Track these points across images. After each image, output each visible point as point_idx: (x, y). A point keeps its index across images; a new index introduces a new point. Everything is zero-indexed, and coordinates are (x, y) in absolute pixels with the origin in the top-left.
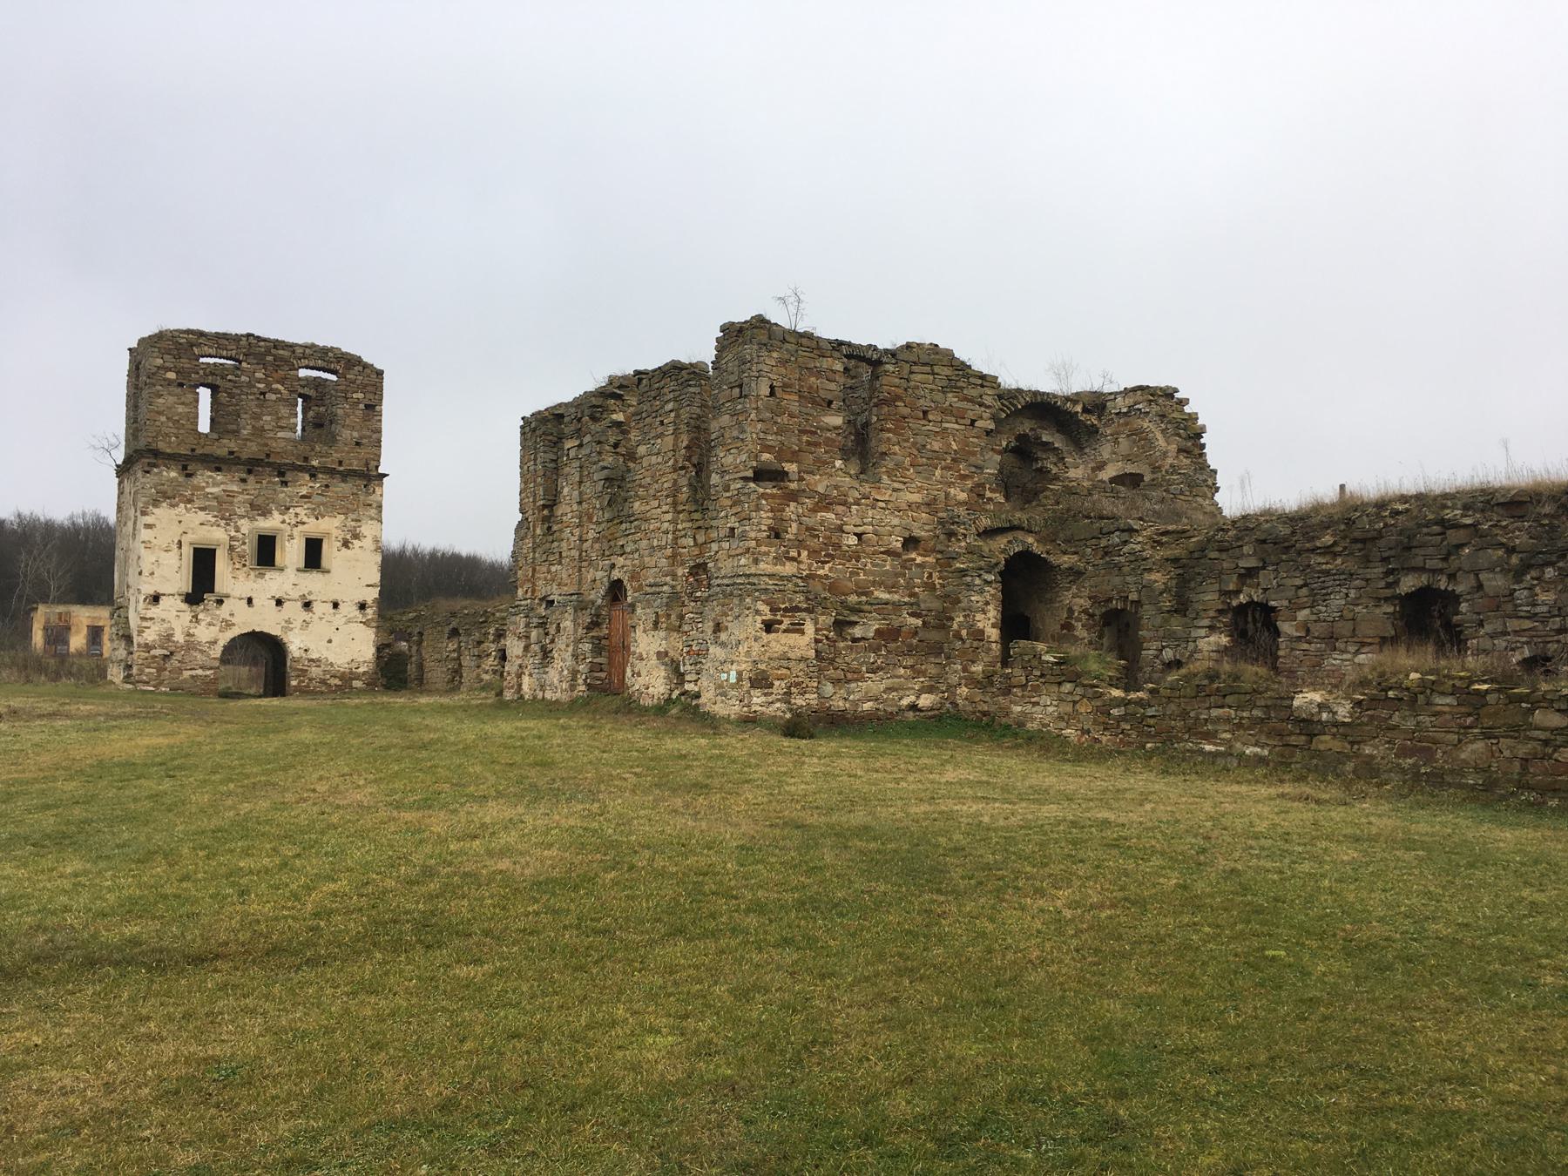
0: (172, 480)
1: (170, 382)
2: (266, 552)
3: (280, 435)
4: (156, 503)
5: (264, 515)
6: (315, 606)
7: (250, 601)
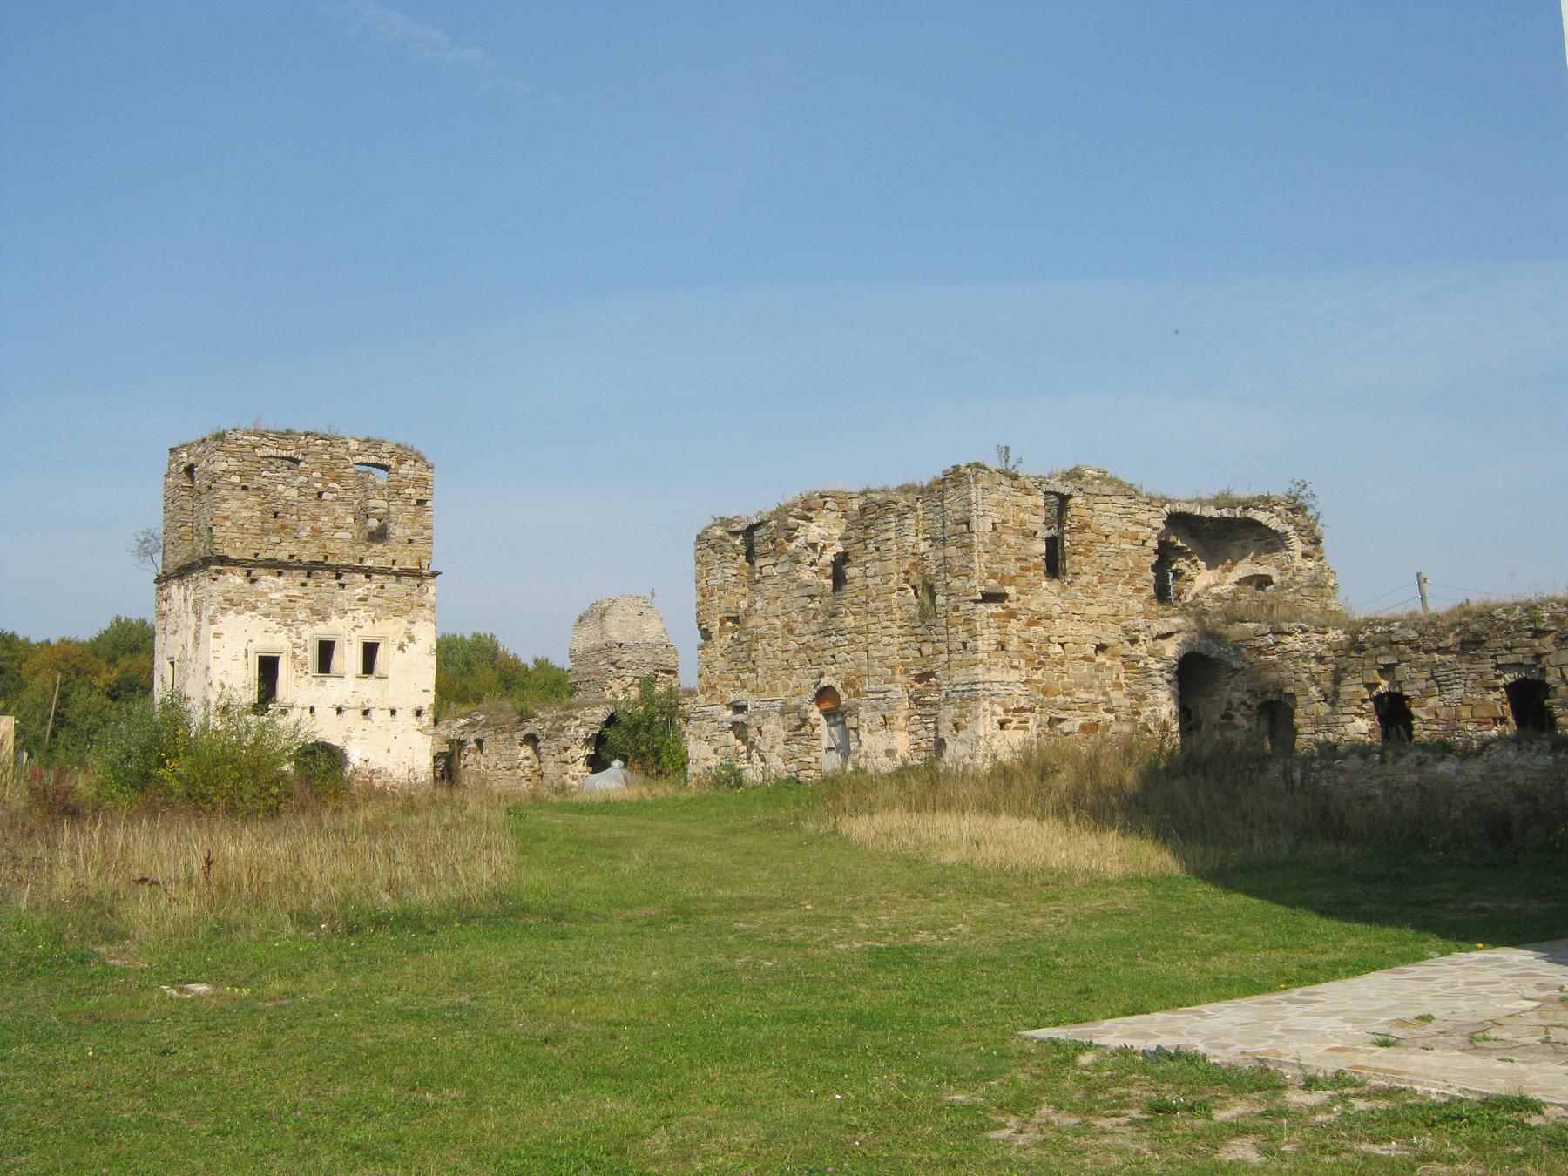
0: (238, 586)
1: (234, 486)
3: (337, 536)
4: (224, 610)
5: (323, 620)
6: (372, 712)
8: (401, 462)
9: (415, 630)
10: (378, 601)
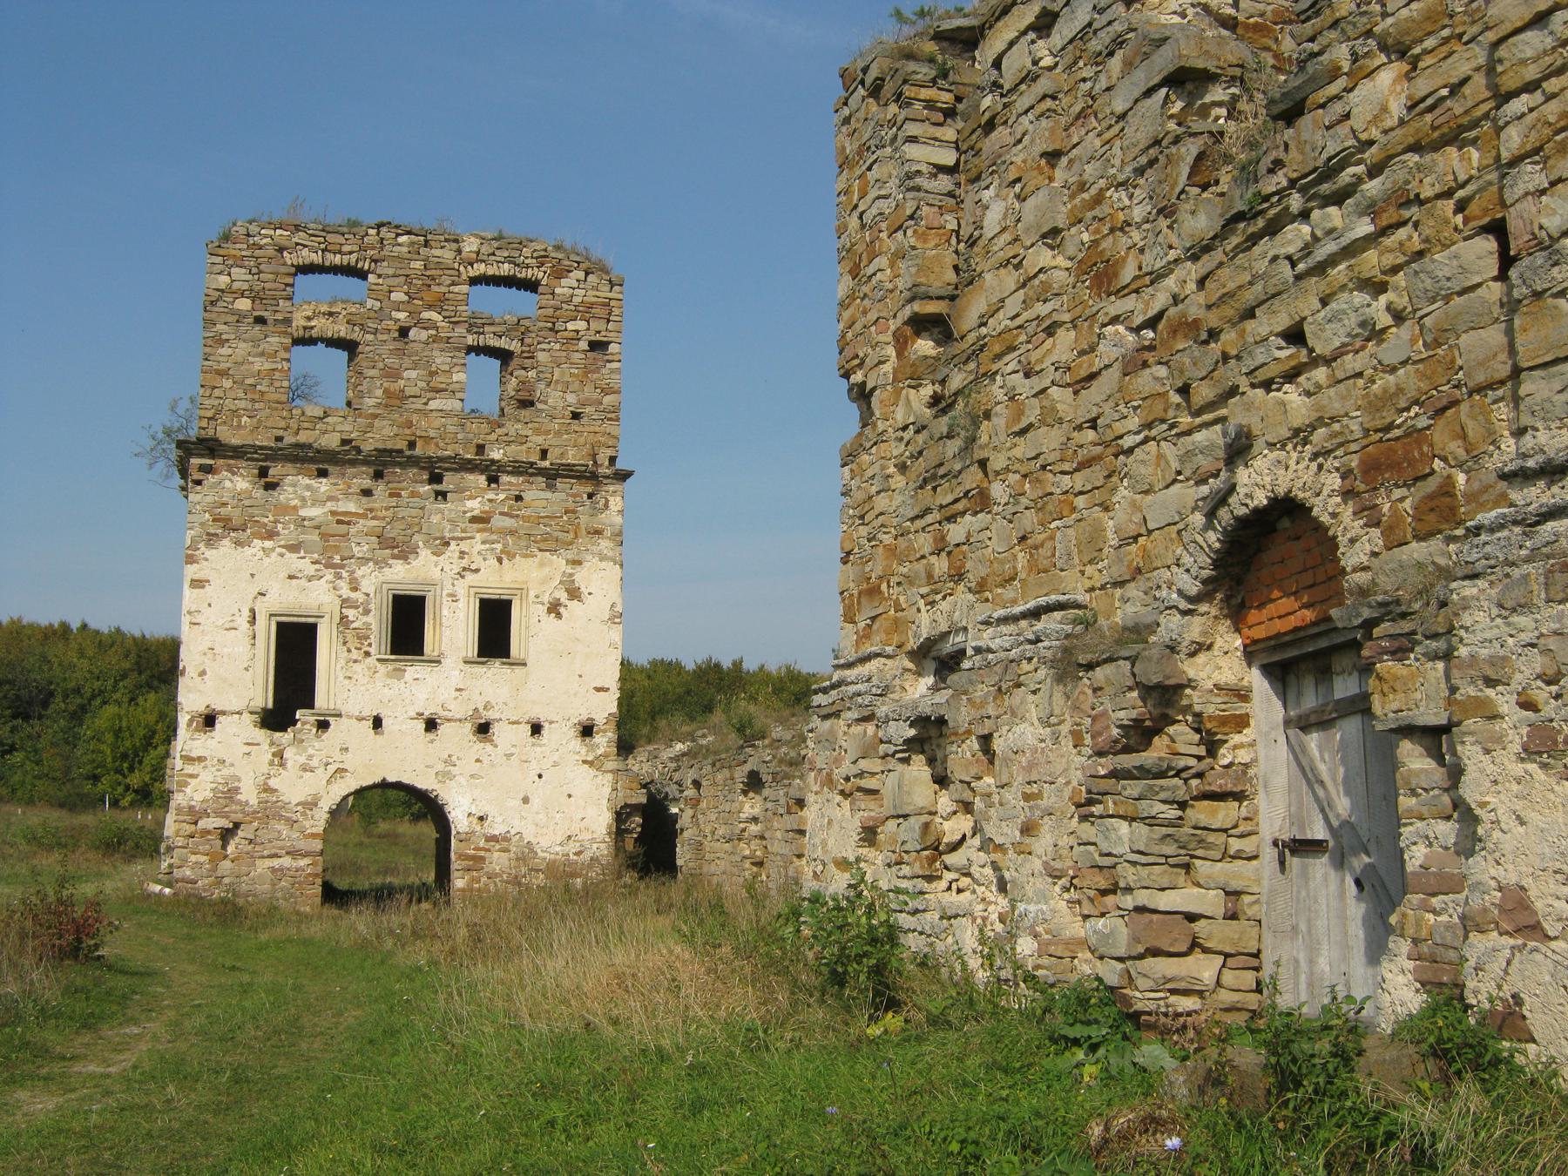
0: (239, 496)
1: (241, 317)
2: (407, 626)
3: (433, 405)
4: (211, 539)
6: (495, 729)
7: (377, 723)
8: (560, 273)
9: (581, 577)
10: (508, 522)
